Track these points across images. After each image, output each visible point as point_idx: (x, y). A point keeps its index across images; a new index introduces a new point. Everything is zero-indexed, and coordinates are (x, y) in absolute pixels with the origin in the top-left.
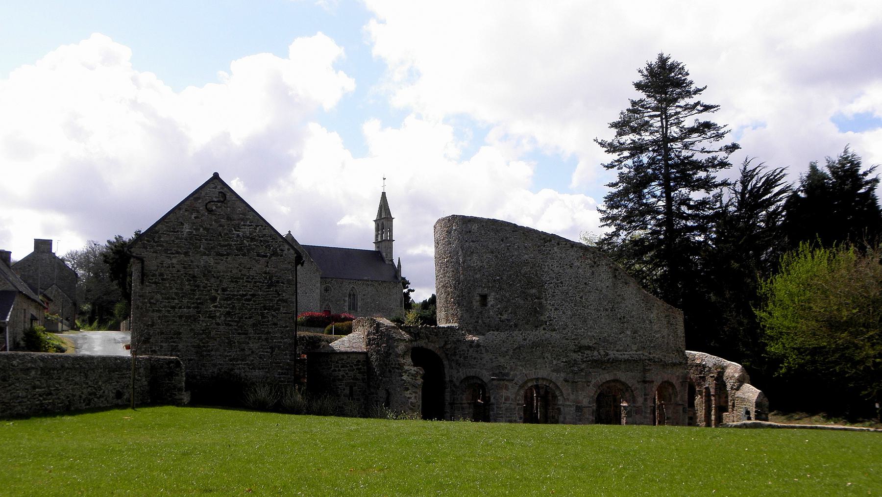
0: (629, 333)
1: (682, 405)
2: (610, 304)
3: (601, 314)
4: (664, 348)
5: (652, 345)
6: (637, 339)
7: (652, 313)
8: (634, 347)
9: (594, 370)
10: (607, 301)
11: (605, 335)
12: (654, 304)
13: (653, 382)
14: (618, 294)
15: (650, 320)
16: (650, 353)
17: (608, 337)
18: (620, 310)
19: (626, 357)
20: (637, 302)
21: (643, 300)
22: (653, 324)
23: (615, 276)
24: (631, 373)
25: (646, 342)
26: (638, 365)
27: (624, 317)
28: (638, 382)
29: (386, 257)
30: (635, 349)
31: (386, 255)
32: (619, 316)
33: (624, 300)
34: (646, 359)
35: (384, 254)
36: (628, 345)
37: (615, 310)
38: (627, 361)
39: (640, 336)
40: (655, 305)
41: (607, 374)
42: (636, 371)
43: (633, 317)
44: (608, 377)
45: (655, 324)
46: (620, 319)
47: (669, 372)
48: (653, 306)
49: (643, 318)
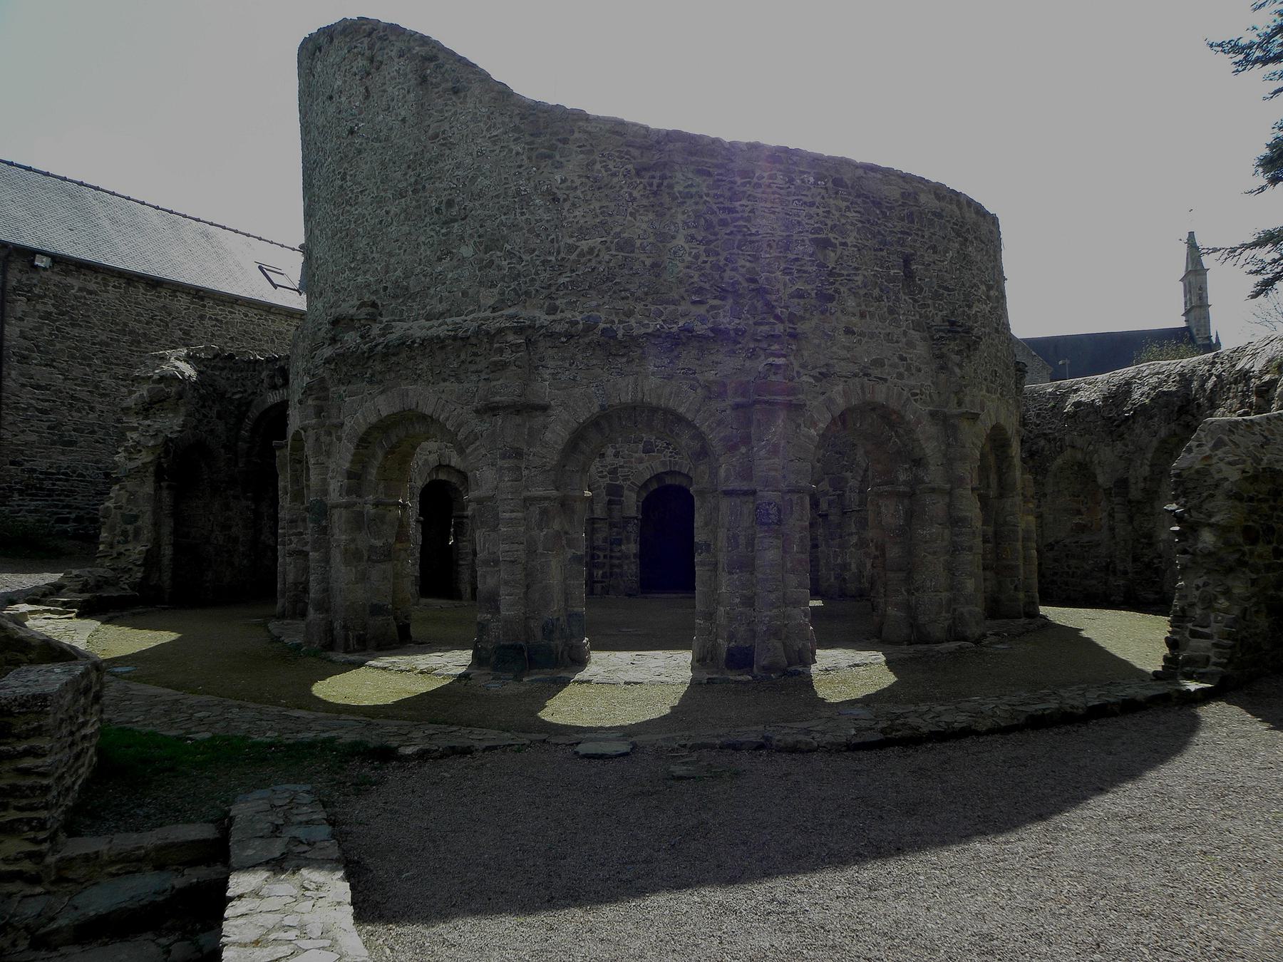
0: (466, 251)
1: (754, 493)
2: (410, 172)
3: (387, 213)
4: (633, 287)
5: (562, 280)
6: (500, 268)
7: (559, 166)
8: (489, 297)
9: (350, 387)
10: (403, 167)
11: (398, 273)
12: (572, 132)
13: (544, 408)
14: (430, 132)
15: (549, 192)
16: (552, 310)
17: (407, 277)
18: (437, 184)
19: (442, 332)
20: (495, 140)
21: (516, 129)
22: (567, 205)
23: (423, 80)
24: (456, 385)
25: (537, 274)
26: (475, 354)
27: (450, 203)
28: (477, 411)
29: (1198, 334)
30: (491, 302)
31: (1198, 330)
32: (434, 204)
33: (451, 146)
34: (500, 331)
35: (1194, 331)
36: (465, 294)
37: (424, 187)
38: (431, 345)
39: (510, 254)
40: (576, 135)
41: (382, 397)
42: (474, 378)
43: (480, 195)
44: (385, 406)
45: (574, 205)
46: (438, 210)
47: (652, 368)
48: (565, 141)
49: (518, 192)
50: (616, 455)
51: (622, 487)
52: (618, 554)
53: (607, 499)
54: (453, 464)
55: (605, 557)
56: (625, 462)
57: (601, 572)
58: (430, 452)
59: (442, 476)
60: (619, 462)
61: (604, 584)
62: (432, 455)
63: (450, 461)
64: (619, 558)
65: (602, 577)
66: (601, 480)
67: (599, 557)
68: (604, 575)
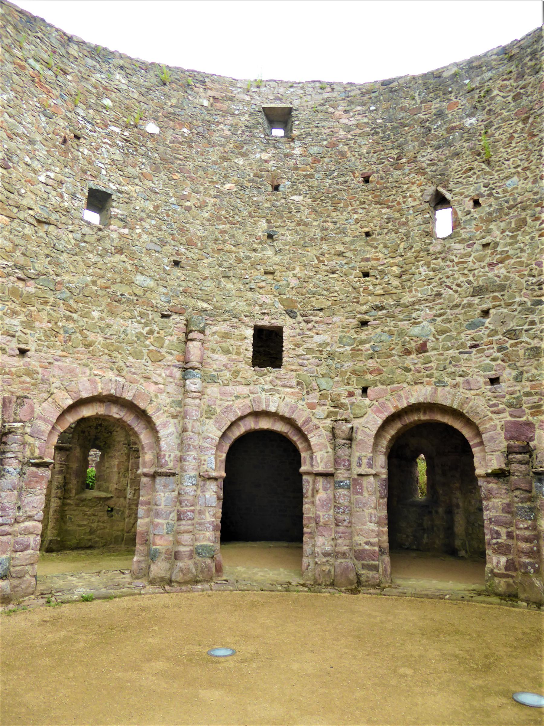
50: (518, 379)
51: (529, 425)
52: (527, 533)
53: (505, 444)
54: (272, 409)
55: (510, 535)
56: (532, 387)
57: (503, 560)
58: (237, 397)
59: (265, 424)
60: (523, 387)
61: (511, 580)
62: (240, 401)
63: (268, 406)
64: (527, 540)
65: (507, 568)
66: (494, 416)
67: (498, 534)
68: (510, 566)
